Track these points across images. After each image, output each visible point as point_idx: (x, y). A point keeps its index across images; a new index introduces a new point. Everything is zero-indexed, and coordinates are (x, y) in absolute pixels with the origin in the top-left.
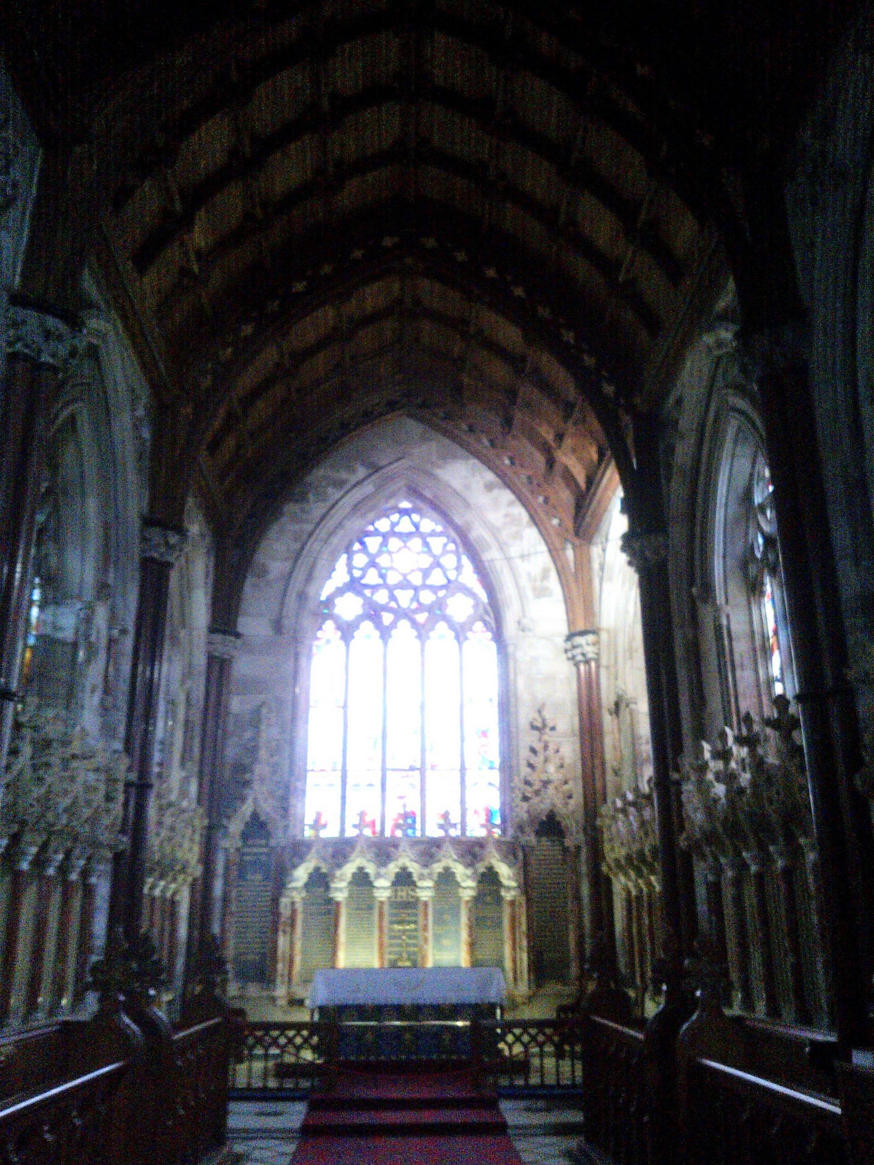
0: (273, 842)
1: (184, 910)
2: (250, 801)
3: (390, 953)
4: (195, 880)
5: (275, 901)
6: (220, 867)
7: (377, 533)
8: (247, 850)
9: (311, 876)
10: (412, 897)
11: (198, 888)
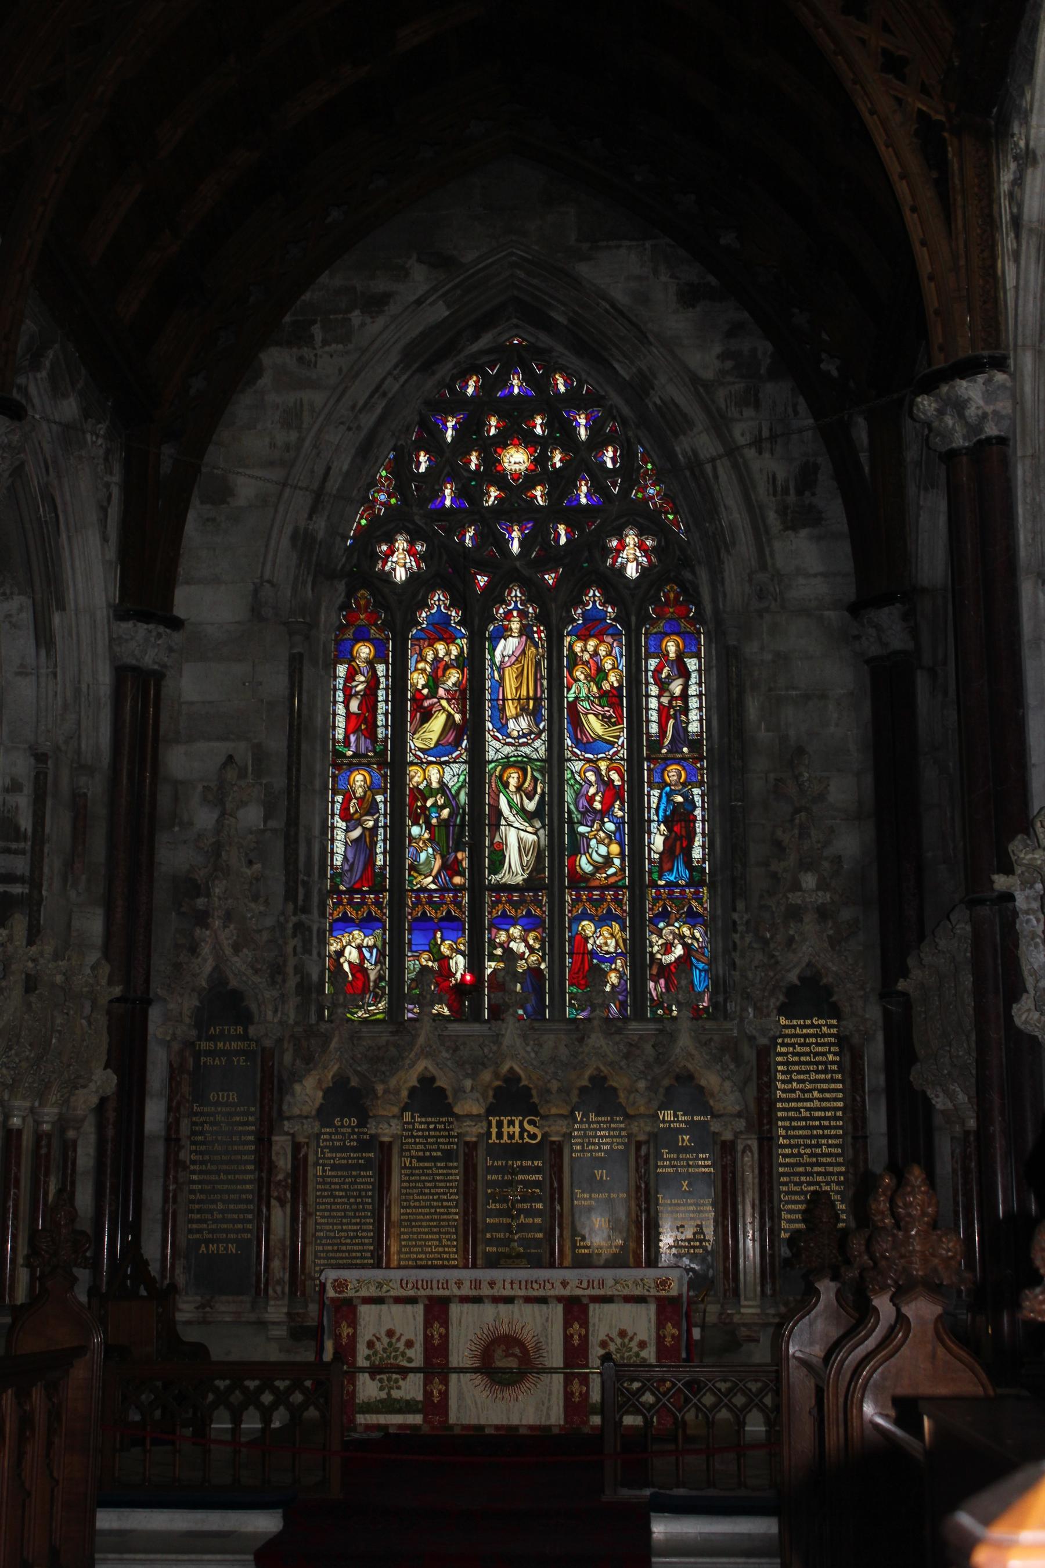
0: (252, 1030)
1: (85, 1157)
2: (206, 949)
3: (490, 1242)
4: (103, 1101)
5: (264, 1143)
7: (457, 404)
8: (204, 1045)
9: (327, 1093)
10: (533, 1136)
11: (111, 1115)
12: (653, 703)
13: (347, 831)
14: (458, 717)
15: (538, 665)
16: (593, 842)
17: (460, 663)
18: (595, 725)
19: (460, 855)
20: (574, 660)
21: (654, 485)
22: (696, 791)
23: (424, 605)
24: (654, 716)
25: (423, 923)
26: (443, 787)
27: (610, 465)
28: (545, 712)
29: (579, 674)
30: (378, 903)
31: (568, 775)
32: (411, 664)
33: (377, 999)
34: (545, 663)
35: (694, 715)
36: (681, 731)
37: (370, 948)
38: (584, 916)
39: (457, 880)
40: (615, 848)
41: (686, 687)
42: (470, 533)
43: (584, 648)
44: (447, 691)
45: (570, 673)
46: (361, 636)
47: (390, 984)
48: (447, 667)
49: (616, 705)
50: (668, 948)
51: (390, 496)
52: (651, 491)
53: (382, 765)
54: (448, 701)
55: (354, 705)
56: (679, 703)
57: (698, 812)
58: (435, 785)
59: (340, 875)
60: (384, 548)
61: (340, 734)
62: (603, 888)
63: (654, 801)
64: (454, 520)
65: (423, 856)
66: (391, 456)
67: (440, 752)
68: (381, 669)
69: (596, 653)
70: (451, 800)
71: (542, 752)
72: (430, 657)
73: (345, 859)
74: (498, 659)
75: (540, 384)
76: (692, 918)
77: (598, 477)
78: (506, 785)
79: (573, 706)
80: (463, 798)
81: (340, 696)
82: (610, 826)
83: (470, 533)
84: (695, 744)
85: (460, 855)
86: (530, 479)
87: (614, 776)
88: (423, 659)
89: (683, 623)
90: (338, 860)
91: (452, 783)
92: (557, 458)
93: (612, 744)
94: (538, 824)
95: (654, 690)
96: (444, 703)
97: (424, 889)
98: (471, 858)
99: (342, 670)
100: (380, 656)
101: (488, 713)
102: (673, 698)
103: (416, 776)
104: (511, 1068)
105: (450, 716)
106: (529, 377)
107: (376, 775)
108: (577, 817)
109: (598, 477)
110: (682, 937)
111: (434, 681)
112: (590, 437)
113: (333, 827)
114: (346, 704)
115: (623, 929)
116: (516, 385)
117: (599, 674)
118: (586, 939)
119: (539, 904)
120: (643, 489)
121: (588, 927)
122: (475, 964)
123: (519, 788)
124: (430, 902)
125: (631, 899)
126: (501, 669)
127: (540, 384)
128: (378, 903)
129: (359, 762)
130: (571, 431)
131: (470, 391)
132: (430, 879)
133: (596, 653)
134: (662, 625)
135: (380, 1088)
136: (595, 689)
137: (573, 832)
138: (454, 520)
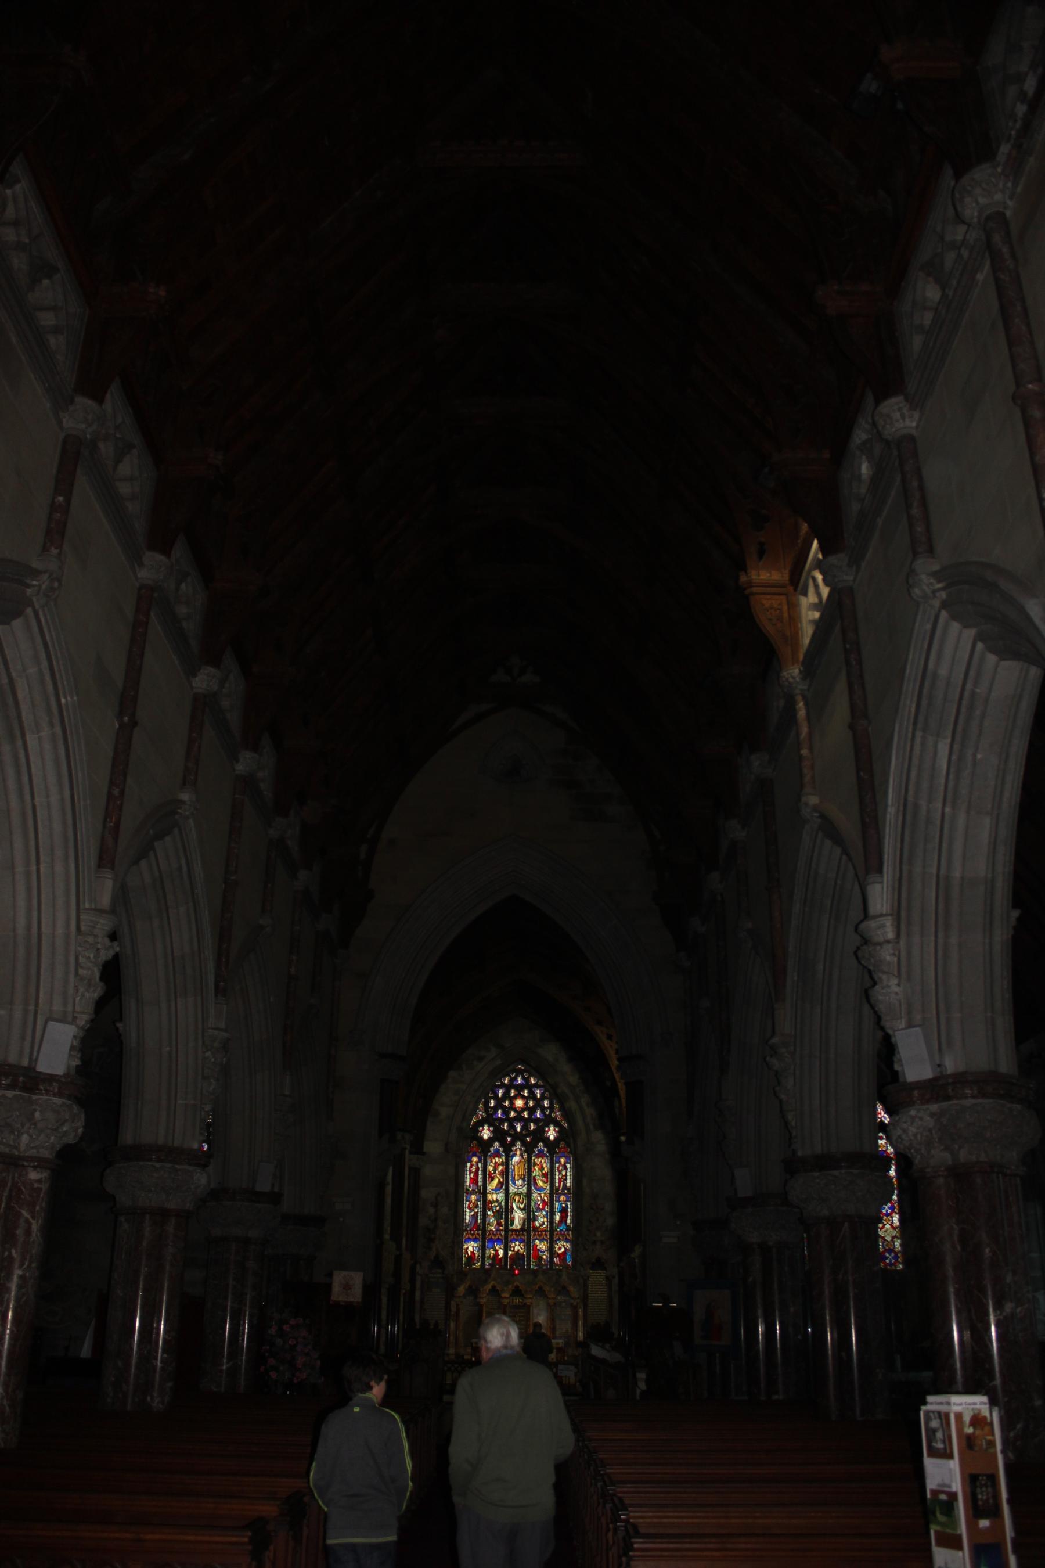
6: (418, 1284)
7: (503, 1085)
12: (557, 1177)
13: (470, 1212)
14: (501, 1180)
15: (525, 1165)
16: (539, 1218)
17: (502, 1164)
18: (540, 1183)
19: (502, 1221)
20: (535, 1164)
21: (558, 1112)
22: (569, 1203)
23: (492, 1146)
24: (557, 1181)
25: (492, 1240)
26: (497, 1201)
27: (546, 1105)
28: (526, 1179)
29: (536, 1168)
30: (478, 1234)
31: (532, 1198)
32: (488, 1164)
33: (478, 1262)
34: (526, 1165)
35: (568, 1181)
36: (565, 1186)
37: (476, 1247)
38: (537, 1239)
39: (501, 1228)
40: (545, 1219)
41: (566, 1172)
42: (506, 1125)
43: (538, 1161)
44: (499, 1172)
45: (534, 1168)
46: (474, 1155)
47: (482, 1257)
48: (499, 1165)
49: (547, 1178)
50: (560, 1249)
51: (483, 1113)
52: (558, 1114)
53: (480, 1193)
54: (499, 1175)
55: (472, 1175)
56: (564, 1177)
57: (569, 1210)
58: (495, 1200)
59: (468, 1225)
60: (481, 1128)
61: (468, 1184)
62: (542, 1231)
63: (557, 1206)
64: (501, 1121)
65: (491, 1220)
66: (483, 1100)
67: (497, 1189)
68: (480, 1165)
69: (541, 1162)
70: (500, 1204)
71: (525, 1191)
72: (494, 1161)
73: (469, 1221)
74: (513, 1163)
75: (526, 1080)
76: (567, 1240)
77: (543, 1109)
78: (515, 1200)
79: (534, 1177)
80: (503, 1204)
81: (468, 1172)
82: (544, 1213)
83: (506, 1125)
84: (569, 1189)
85: (502, 1221)
86: (523, 1110)
87: (546, 1198)
88: (492, 1162)
89: (566, 1153)
90: (467, 1221)
91: (500, 1199)
92: (531, 1104)
93: (545, 1189)
94: (524, 1212)
95: (557, 1173)
96: (498, 1176)
97: (492, 1230)
98: (505, 1221)
99: (468, 1165)
100: (480, 1161)
101: (510, 1179)
102: (563, 1176)
103: (490, 1197)
104: (517, 1285)
105: (499, 1180)
106: (523, 1078)
107: (478, 1196)
108: (535, 1210)
109: (543, 1109)
110: (564, 1246)
111: (495, 1169)
112: (540, 1097)
113: (466, 1211)
114: (470, 1175)
115: (547, 1243)
116: (520, 1080)
117: (542, 1168)
118: (537, 1246)
119: (523, 1235)
120: (555, 1113)
121: (537, 1242)
122: (506, 1253)
123: (519, 1201)
124: (493, 1234)
125: (550, 1234)
126: (514, 1166)
127: (526, 1080)
128: (478, 1234)
129: (473, 1192)
130: (535, 1095)
131: (506, 1081)
132: (493, 1227)
133: (541, 1162)
134: (560, 1154)
135: (481, 1289)
136: (541, 1173)
137: (534, 1214)
138: (501, 1121)
